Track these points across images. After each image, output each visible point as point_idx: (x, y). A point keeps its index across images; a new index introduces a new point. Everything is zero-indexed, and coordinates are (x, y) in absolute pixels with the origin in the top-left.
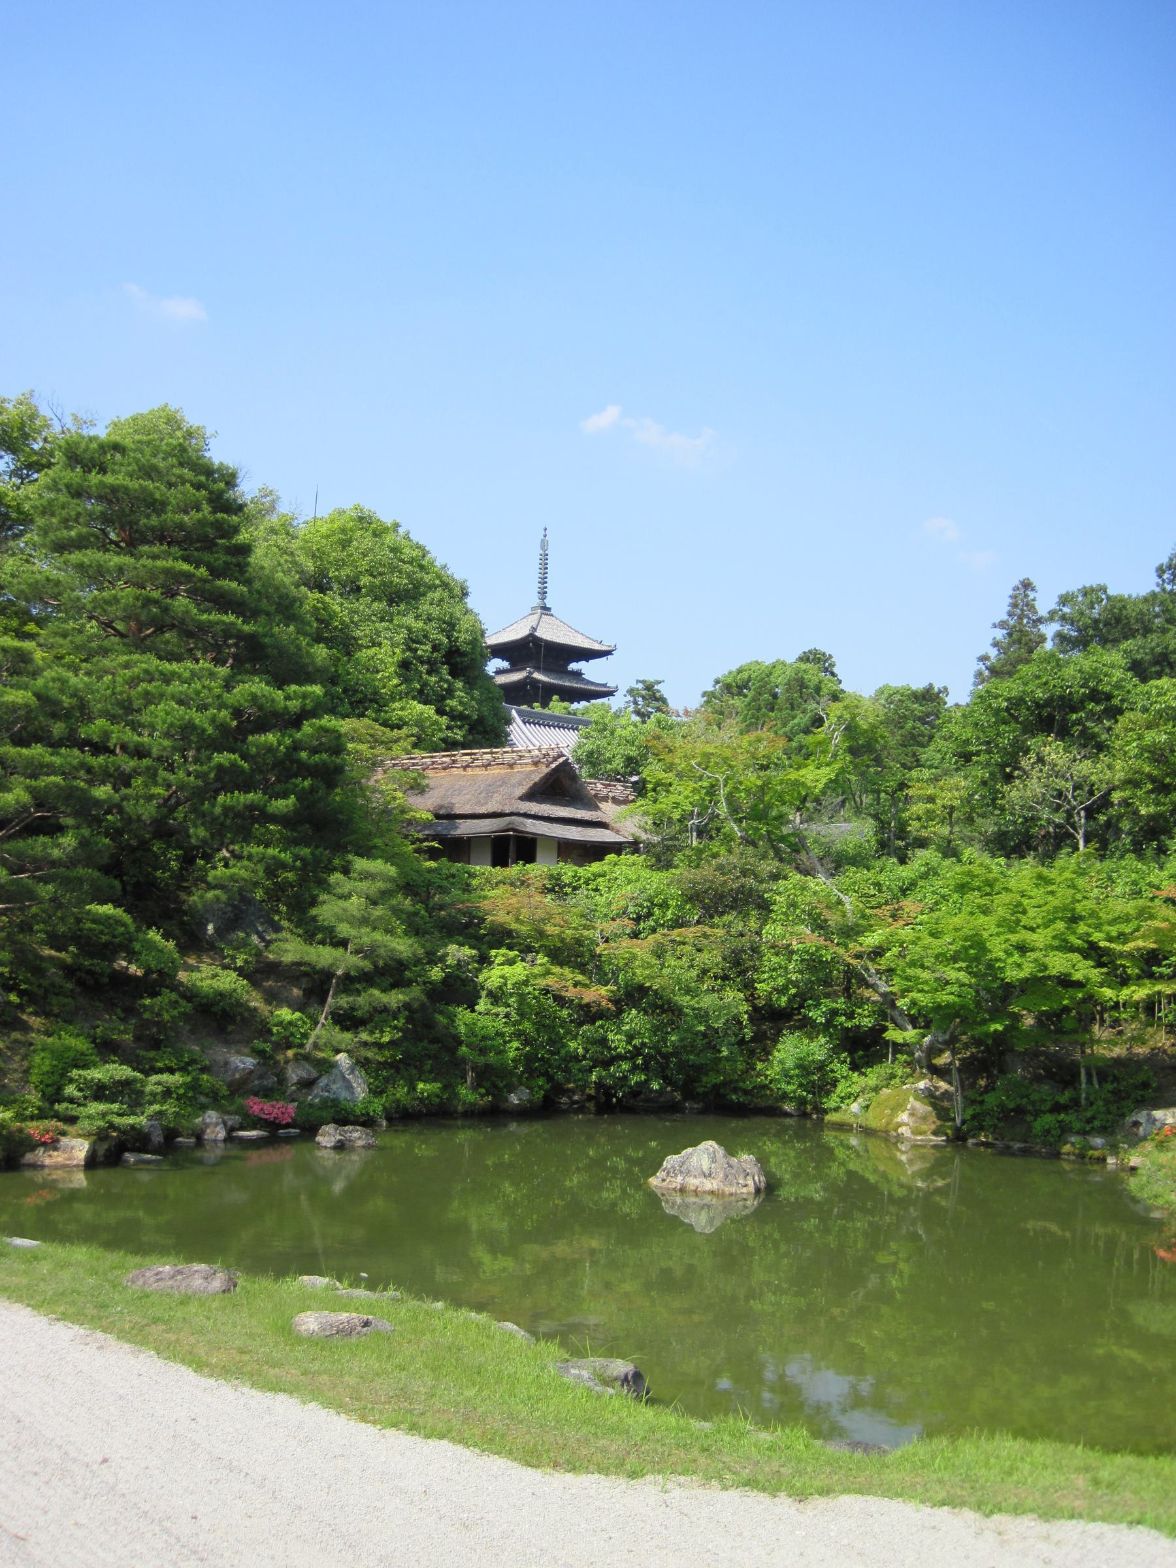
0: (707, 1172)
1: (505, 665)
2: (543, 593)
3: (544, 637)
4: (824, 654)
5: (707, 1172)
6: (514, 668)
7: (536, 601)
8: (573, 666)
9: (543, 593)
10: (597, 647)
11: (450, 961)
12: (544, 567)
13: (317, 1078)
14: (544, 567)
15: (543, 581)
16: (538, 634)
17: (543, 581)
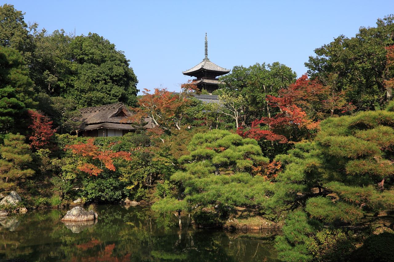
0: (74, 215)
1: (196, 78)
2: (206, 54)
3: (206, 68)
4: (288, 68)
5: (74, 215)
6: (198, 79)
7: (204, 57)
8: (217, 77)
9: (206, 54)
10: (224, 70)
11: (53, 164)
12: (206, 46)
13: (4, 198)
14: (206, 46)
15: (206, 50)
16: (204, 68)
17: (206, 50)
